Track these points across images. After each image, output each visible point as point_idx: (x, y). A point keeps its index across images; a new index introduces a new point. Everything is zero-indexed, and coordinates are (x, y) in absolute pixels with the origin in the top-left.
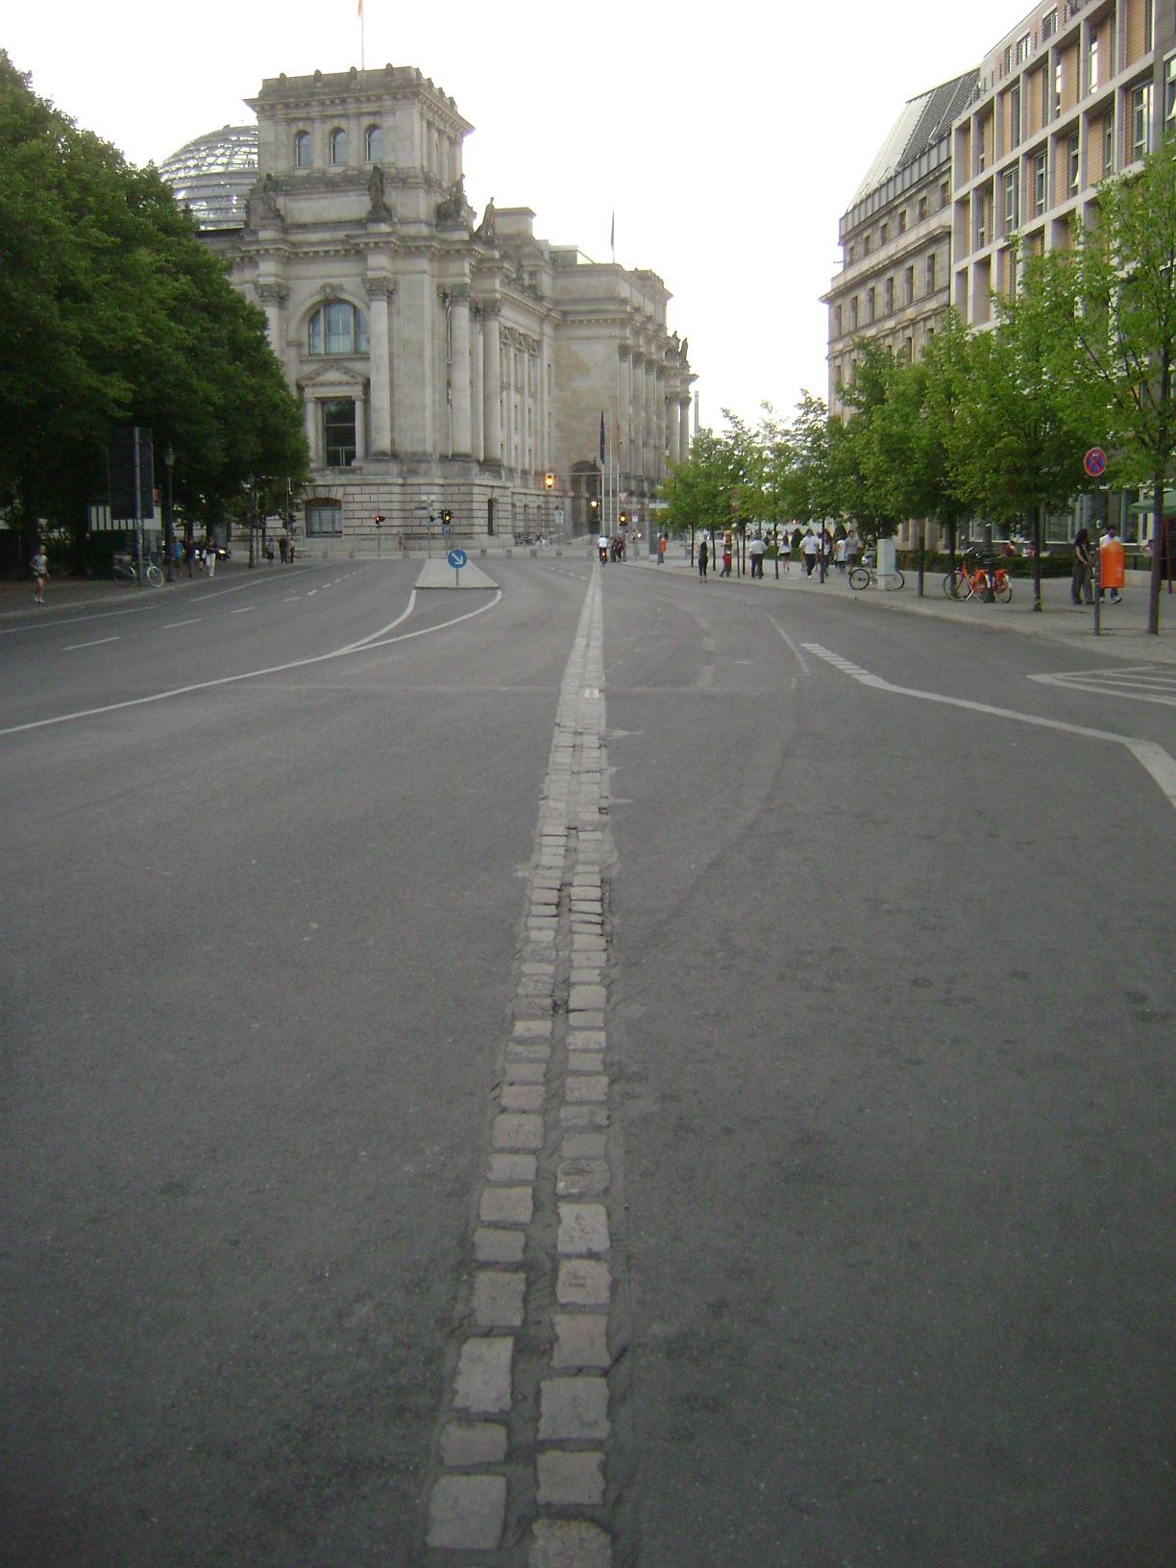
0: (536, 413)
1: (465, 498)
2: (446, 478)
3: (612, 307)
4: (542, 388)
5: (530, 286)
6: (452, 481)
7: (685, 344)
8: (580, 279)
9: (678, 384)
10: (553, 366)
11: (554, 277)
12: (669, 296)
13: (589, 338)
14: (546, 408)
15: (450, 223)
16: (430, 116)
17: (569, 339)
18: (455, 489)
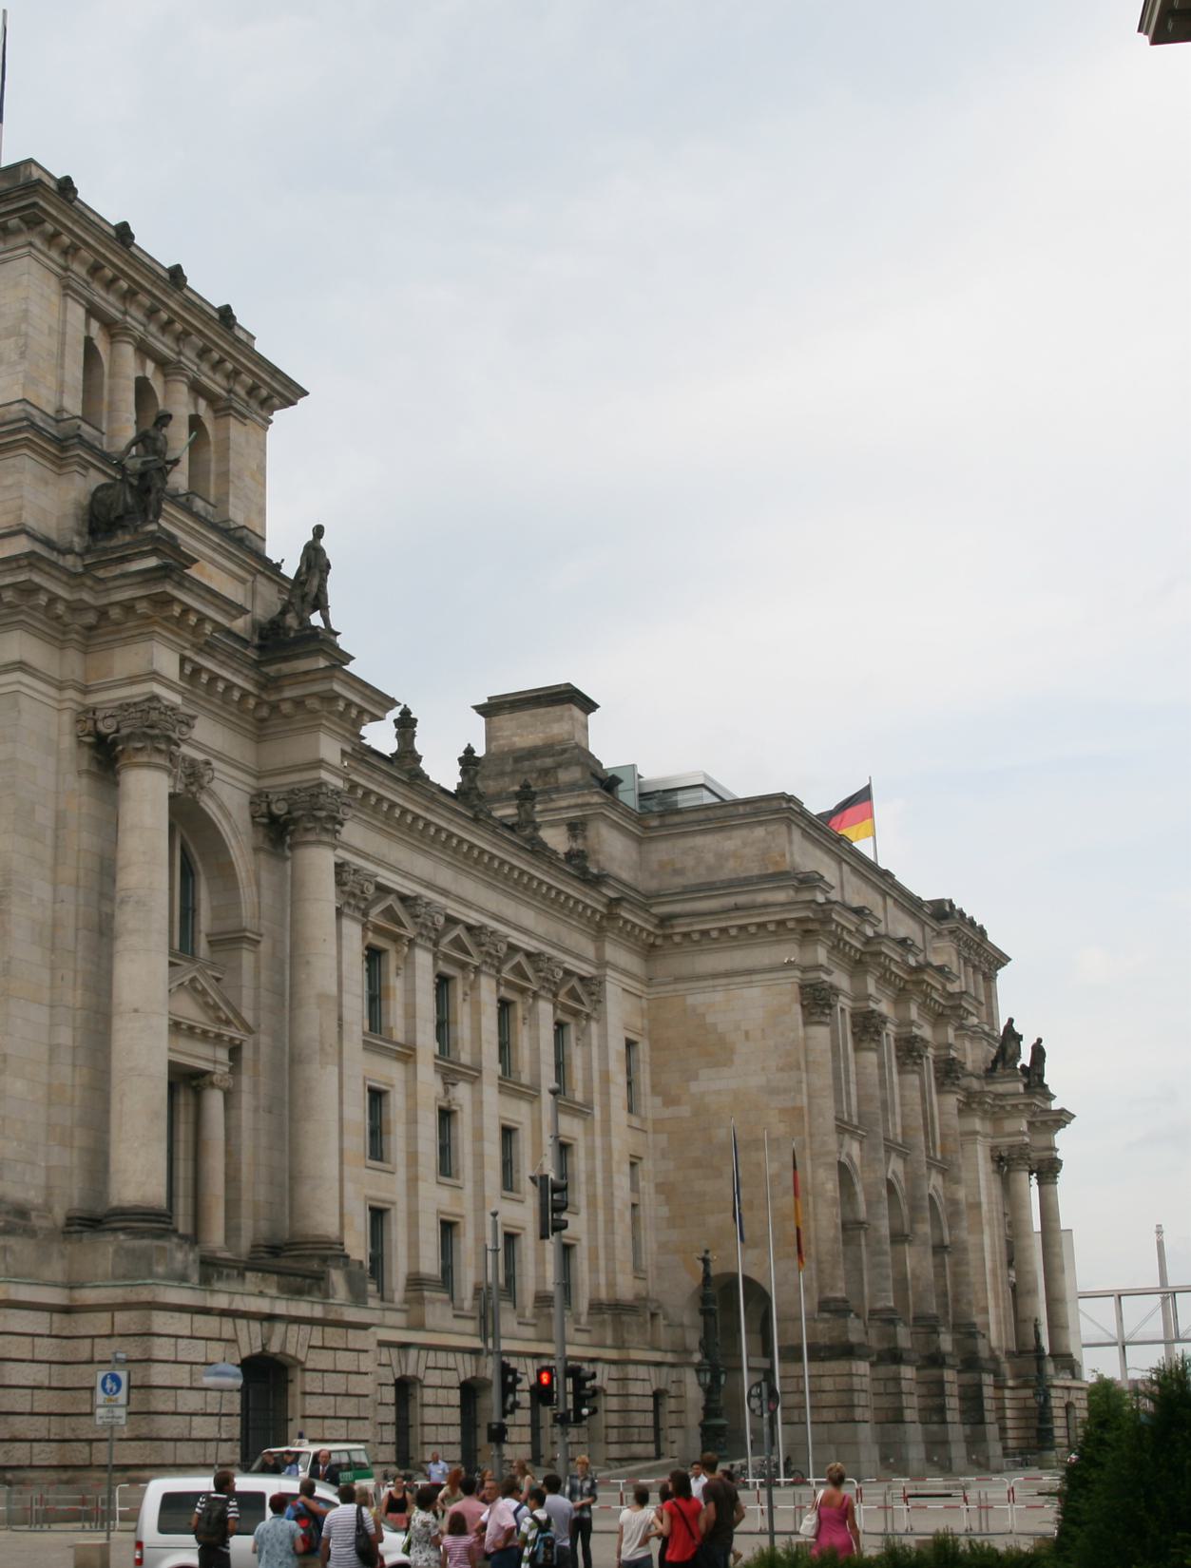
0: (591, 1153)
1: (133, 1349)
2: (71, 1286)
3: (781, 896)
4: (606, 1092)
5: (570, 856)
6: (88, 1296)
7: (1038, 1052)
8: (699, 841)
9: (1024, 1127)
10: (644, 1049)
11: (639, 841)
12: (1002, 960)
13: (728, 974)
14: (616, 1143)
15: (123, 538)
16: (109, 303)
17: (678, 979)
18: (100, 1323)
